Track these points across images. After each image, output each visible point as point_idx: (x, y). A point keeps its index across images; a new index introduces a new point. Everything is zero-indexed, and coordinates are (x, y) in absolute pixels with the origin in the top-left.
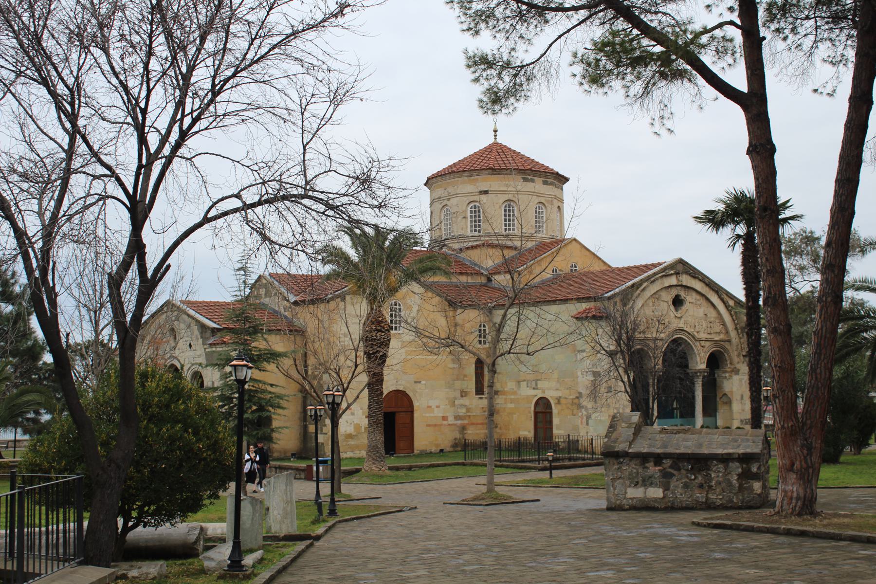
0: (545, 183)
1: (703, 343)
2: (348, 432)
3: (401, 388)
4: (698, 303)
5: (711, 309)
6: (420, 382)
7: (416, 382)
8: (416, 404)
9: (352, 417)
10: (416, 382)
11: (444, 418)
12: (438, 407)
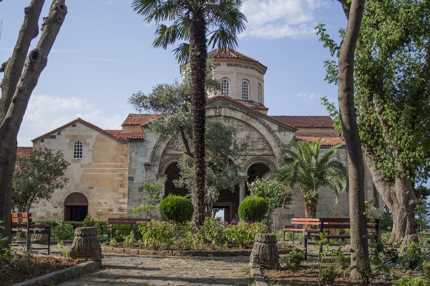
0: (229, 65)
2: (42, 216)
3: (79, 191)
4: (240, 128)
5: (255, 133)
6: (93, 188)
7: (90, 188)
8: (90, 201)
9: (45, 207)
10: (90, 188)
11: (111, 210)
12: (105, 203)
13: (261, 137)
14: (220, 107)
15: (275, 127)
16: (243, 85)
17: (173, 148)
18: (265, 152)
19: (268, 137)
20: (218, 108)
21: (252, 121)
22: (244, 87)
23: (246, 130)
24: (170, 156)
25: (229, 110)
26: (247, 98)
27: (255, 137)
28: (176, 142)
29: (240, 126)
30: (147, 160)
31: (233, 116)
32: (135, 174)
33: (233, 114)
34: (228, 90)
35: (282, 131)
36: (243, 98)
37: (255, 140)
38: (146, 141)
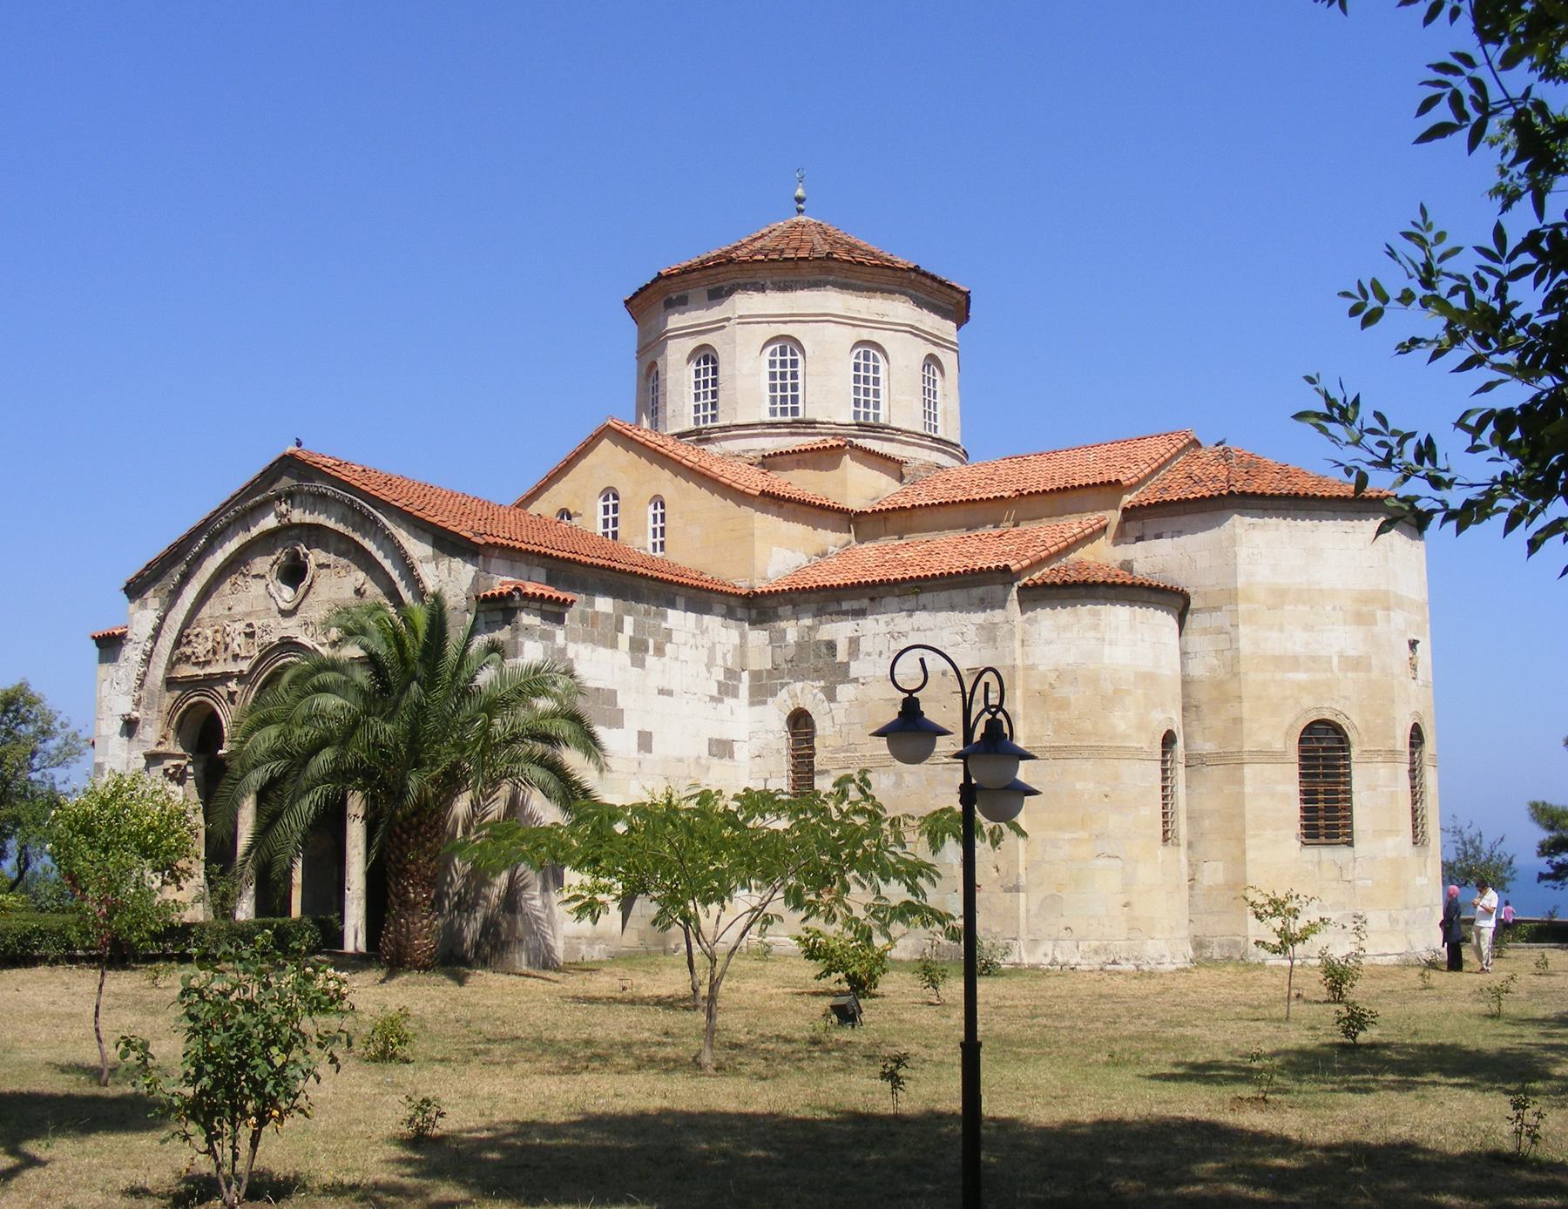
15: (418, 549)
16: (772, 364)
22: (778, 369)
26: (795, 411)
30: (125, 706)
32: (106, 754)
34: (714, 394)
36: (773, 412)
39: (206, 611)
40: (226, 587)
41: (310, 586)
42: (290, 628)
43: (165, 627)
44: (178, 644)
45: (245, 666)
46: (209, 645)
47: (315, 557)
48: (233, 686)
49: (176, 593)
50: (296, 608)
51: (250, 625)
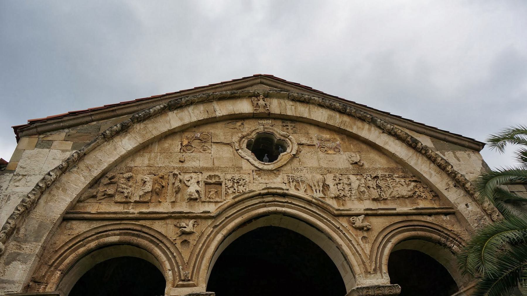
1: (359, 222)
4: (329, 144)
5: (373, 155)
13: (393, 165)
14: (267, 96)
15: (425, 141)
17: (111, 196)
18: (422, 204)
19: (416, 164)
20: (262, 96)
21: (358, 128)
23: (346, 150)
24: (95, 225)
25: (291, 103)
27: (379, 166)
28: (128, 179)
29: (329, 140)
31: (306, 115)
33: (303, 111)
35: (448, 150)
37: (380, 173)
38: (12, 171)
39: (141, 162)
40: (175, 144)
41: (294, 156)
42: (277, 182)
43: (82, 165)
44: (96, 182)
45: (212, 209)
46: (148, 187)
47: (294, 139)
48: (189, 225)
49: (108, 138)
50: (278, 169)
51: (210, 177)
